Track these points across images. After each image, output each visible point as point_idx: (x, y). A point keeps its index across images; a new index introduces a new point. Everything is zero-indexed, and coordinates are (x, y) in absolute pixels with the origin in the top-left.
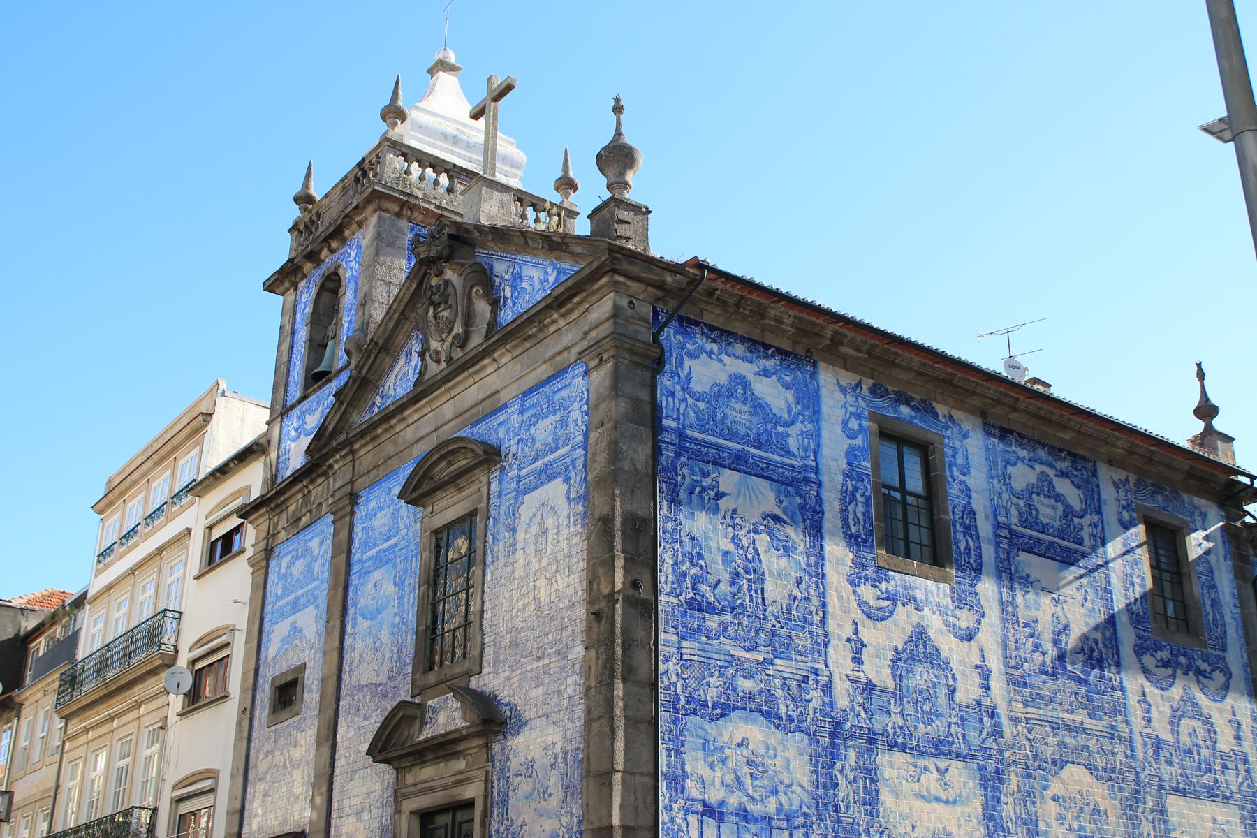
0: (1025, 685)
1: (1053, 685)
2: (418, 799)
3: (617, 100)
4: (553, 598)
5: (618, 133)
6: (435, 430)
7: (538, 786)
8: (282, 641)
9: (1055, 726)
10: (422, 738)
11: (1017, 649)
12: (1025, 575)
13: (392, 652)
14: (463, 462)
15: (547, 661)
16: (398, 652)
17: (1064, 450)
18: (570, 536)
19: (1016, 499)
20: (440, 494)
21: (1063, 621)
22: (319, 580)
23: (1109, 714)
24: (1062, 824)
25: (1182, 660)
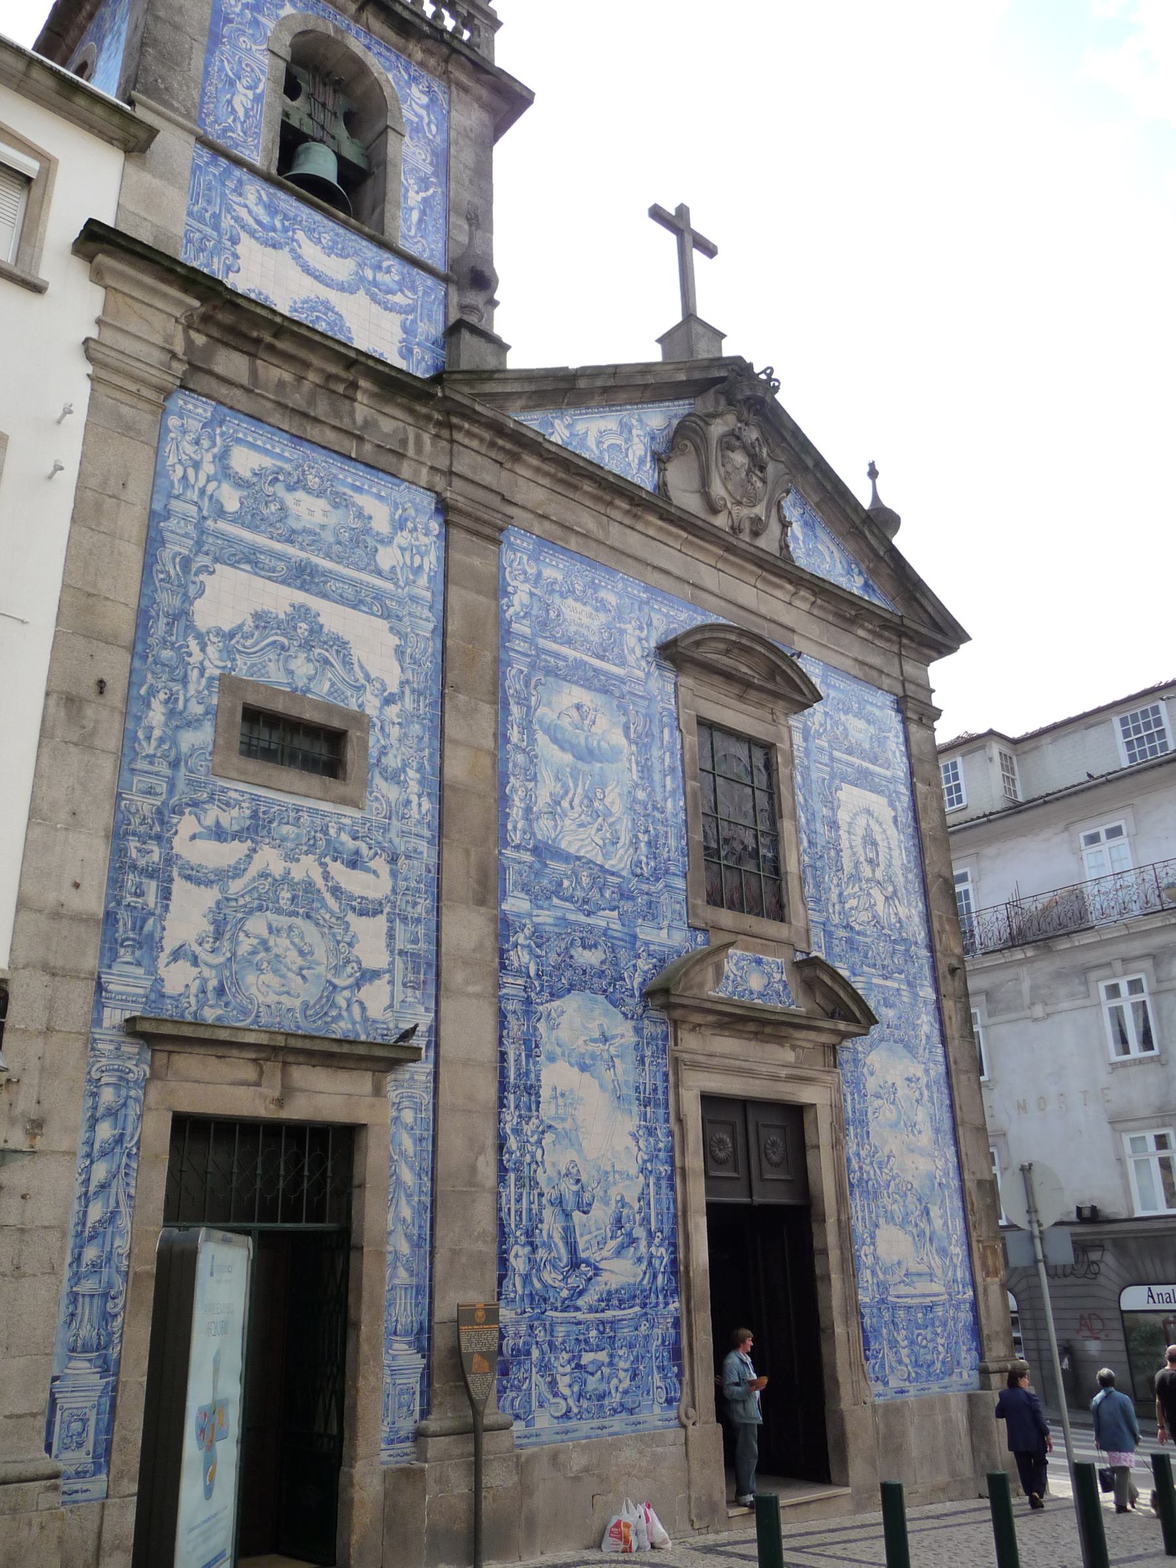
2: (717, 1077)
3: (872, 465)
4: (893, 921)
5: (876, 498)
6: (694, 585)
7: (904, 1117)
8: (257, 616)
10: (721, 995)
13: (636, 837)
14: (744, 669)
15: (896, 985)
16: (649, 843)
18: (907, 868)
20: (717, 680)
22: (396, 584)
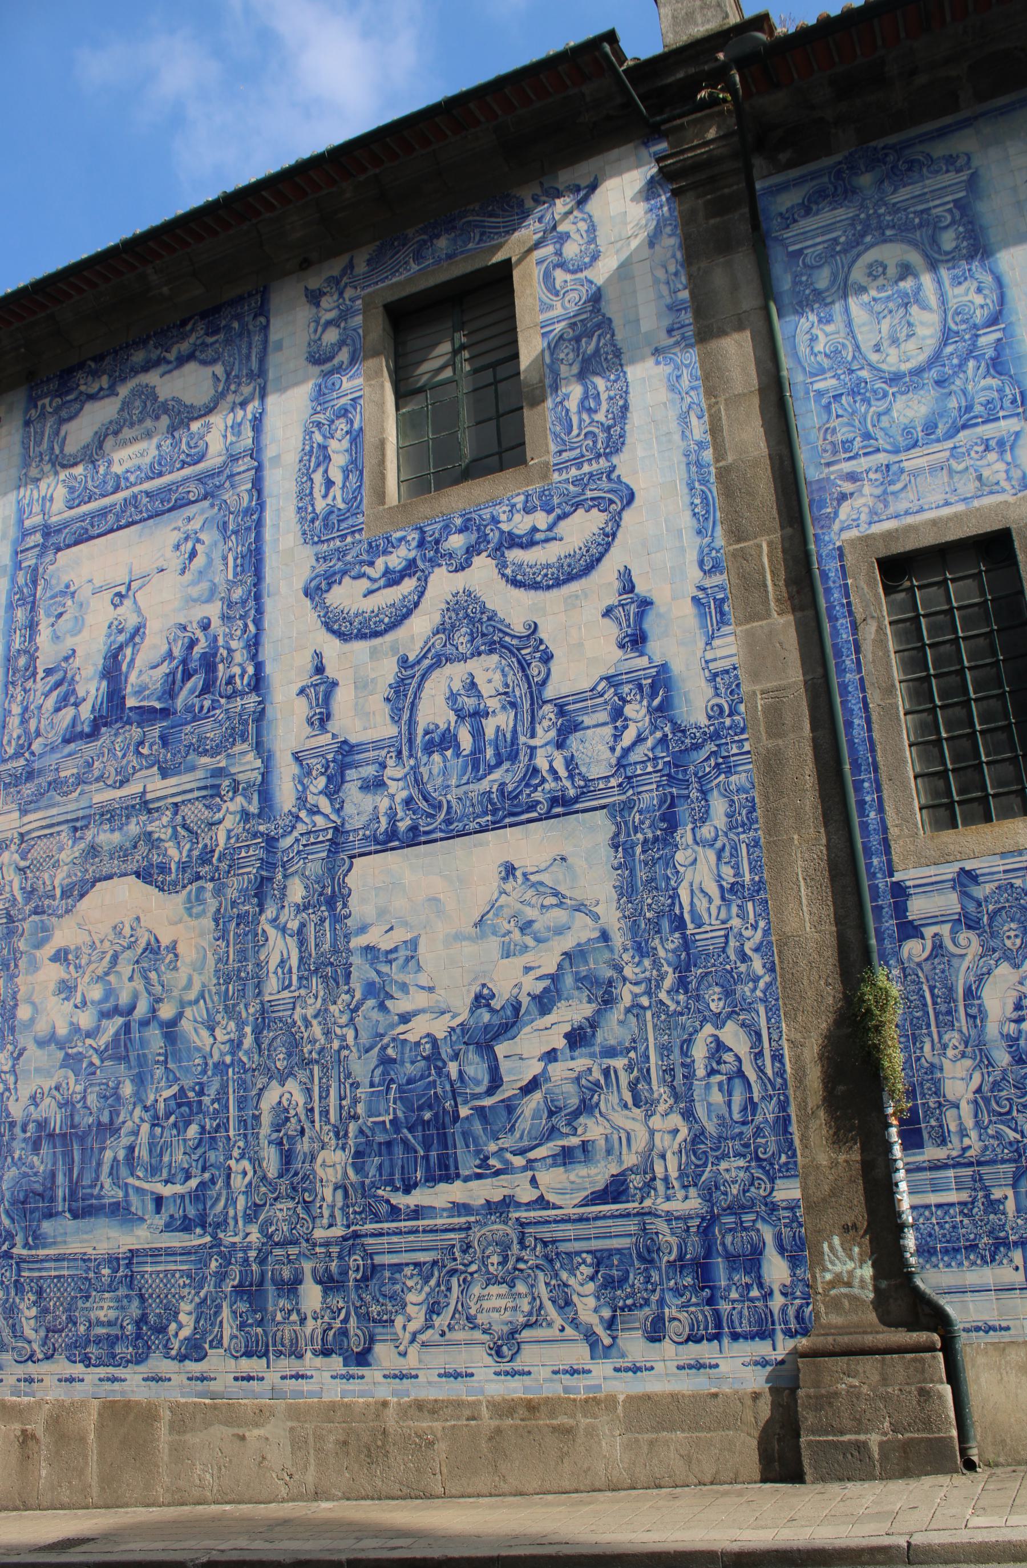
0: (30, 775)
1: (90, 749)
9: (78, 824)
11: (22, 723)
12: (62, 587)
17: (190, 319)
19: (67, 472)
21: (132, 621)
23: (214, 752)
24: (67, 999)
25: (456, 542)
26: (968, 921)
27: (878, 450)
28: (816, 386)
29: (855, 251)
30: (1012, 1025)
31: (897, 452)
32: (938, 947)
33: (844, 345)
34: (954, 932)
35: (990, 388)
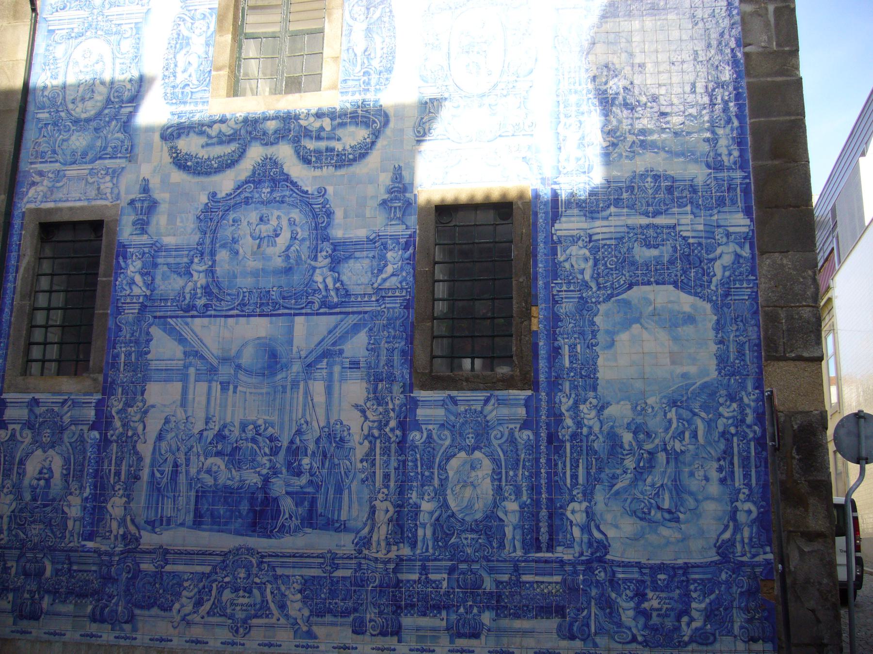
26: (29, 425)
27: (56, 161)
28: (39, 116)
29: (80, 39)
30: (36, 481)
31: (65, 164)
32: (13, 435)
33: (58, 95)
34: (22, 429)
35: (118, 139)
